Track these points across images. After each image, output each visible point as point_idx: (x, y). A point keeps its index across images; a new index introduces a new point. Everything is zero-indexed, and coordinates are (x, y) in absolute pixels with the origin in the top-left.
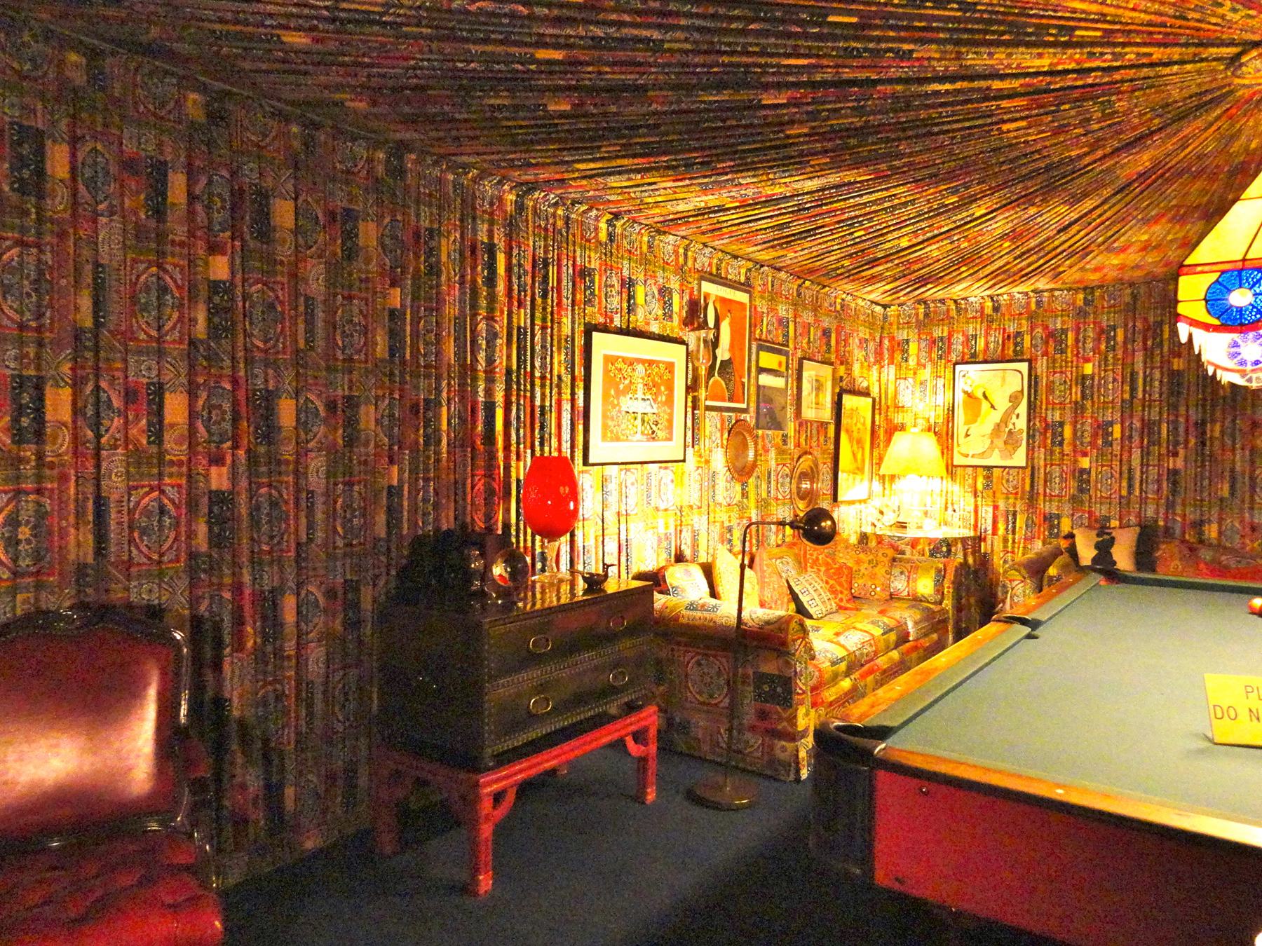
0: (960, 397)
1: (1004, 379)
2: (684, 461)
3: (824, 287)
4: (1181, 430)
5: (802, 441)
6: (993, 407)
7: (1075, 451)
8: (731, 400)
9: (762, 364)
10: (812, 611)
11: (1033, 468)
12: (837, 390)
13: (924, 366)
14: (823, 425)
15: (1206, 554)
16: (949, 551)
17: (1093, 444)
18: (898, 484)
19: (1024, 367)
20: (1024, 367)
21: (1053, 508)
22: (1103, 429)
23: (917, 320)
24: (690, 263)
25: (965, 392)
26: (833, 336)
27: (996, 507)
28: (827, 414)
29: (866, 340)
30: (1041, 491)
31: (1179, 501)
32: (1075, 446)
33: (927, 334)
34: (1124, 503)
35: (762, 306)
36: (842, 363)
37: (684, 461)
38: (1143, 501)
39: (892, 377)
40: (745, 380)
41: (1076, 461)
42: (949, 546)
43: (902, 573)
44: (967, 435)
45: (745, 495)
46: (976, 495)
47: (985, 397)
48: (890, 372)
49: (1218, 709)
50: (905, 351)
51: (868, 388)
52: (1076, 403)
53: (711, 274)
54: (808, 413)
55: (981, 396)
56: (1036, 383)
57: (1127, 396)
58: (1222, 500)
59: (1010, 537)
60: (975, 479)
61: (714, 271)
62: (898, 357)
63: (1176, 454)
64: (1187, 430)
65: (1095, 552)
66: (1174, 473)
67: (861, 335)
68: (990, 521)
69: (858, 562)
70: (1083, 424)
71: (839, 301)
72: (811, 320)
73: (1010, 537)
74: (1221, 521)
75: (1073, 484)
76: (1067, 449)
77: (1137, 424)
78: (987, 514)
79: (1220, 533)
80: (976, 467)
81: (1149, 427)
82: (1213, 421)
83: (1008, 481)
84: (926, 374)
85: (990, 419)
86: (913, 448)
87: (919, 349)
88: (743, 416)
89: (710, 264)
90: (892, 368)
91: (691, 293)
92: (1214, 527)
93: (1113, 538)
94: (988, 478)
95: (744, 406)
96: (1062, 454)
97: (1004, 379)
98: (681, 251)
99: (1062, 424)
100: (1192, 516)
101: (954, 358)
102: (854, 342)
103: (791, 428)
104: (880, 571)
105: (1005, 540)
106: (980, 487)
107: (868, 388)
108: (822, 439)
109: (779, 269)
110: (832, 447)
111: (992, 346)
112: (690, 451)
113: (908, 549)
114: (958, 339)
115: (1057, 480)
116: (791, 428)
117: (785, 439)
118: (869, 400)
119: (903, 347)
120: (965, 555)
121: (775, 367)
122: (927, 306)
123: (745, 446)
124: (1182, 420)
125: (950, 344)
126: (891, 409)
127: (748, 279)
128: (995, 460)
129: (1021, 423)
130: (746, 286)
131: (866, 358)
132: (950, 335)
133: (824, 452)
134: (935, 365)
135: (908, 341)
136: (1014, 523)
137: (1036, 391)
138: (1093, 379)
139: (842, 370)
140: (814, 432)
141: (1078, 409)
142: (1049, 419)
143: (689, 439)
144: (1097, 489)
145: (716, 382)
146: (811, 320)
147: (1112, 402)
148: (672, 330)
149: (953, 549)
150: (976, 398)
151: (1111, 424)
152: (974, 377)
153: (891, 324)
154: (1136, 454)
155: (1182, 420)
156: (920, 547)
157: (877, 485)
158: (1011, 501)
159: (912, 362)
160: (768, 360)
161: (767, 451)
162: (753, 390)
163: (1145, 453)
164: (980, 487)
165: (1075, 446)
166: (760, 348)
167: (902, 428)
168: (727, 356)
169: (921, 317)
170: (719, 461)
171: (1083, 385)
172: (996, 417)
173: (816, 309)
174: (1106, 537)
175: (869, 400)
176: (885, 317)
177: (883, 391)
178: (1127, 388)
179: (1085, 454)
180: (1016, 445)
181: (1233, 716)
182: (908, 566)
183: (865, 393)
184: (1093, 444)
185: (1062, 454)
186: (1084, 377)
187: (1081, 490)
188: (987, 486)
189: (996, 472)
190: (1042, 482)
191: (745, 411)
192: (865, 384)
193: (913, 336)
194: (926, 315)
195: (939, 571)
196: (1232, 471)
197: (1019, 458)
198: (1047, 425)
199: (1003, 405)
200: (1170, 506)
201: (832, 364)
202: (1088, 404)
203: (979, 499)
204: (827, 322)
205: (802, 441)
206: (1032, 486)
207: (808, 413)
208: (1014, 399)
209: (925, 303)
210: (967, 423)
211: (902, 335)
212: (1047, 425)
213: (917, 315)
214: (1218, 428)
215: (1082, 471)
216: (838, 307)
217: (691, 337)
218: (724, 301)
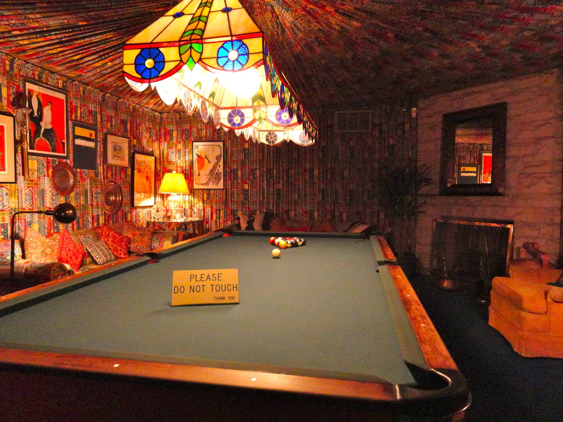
0: (195, 157)
1: (213, 149)
2: (15, 183)
3: (120, 98)
4: (281, 172)
5: (109, 175)
6: (209, 162)
7: (242, 182)
8: (52, 151)
9: (76, 133)
10: (98, 261)
11: (226, 190)
12: (132, 151)
13: (180, 143)
14: (123, 169)
15: (288, 224)
16: (186, 228)
17: (249, 179)
18: (169, 198)
19: (221, 144)
20: (221, 144)
21: (235, 207)
22: (252, 171)
23: (176, 121)
24: (16, 71)
25: (198, 155)
26: (129, 124)
27: (212, 208)
28: (125, 163)
29: (150, 128)
30: (230, 200)
31: (281, 202)
32: (242, 179)
33: (181, 127)
34: (261, 204)
35: (76, 103)
36: (134, 138)
37: (15, 183)
38: (268, 203)
39: (166, 147)
40: (65, 141)
41: (243, 186)
43: (157, 239)
44: (199, 175)
46: (203, 203)
47: (207, 158)
48: (164, 146)
49: (176, 288)
50: (171, 135)
51: (152, 151)
52: (242, 160)
53: (34, 79)
54: (111, 161)
55: (204, 157)
56: (227, 152)
57: (261, 158)
58: (295, 201)
59: (218, 221)
60: (203, 195)
61: (37, 78)
62: (168, 138)
63: (279, 183)
64: (283, 172)
65: (247, 225)
66: (278, 190)
67: (147, 125)
68: (210, 214)
69: (134, 235)
70: (245, 170)
71: (131, 107)
72: (113, 114)
73: (218, 221)
74: (295, 210)
75: (242, 197)
76: (239, 181)
77: (265, 170)
78: (208, 210)
79: (295, 215)
80: (203, 189)
81: (269, 171)
82: (292, 169)
83: (216, 196)
84: (180, 146)
85: (208, 167)
86: (173, 182)
87: (177, 135)
88: (64, 161)
89: (33, 74)
90: (166, 144)
91: (18, 86)
92: (293, 212)
93: (254, 219)
94: (209, 194)
95: (65, 155)
96: (237, 183)
97: (213, 149)
99: (237, 170)
100: (286, 207)
101: (192, 139)
102: (143, 128)
103: (100, 169)
104: (146, 239)
105: (216, 222)
106: (205, 198)
107: (152, 151)
108: (123, 176)
109: (87, 84)
110: (130, 180)
111: (208, 134)
112: (21, 178)
113: (167, 228)
114: (194, 130)
115: (236, 194)
116: (100, 169)
117: (97, 175)
118: (154, 158)
119: (168, 133)
120: (194, 229)
121: (88, 136)
122: (180, 114)
123: (67, 177)
124: (281, 168)
125: (191, 133)
126: (166, 163)
127: (63, 86)
128: (211, 186)
129: (221, 170)
130: (63, 90)
131: (150, 137)
132: (191, 128)
133: (124, 181)
134: (185, 142)
135: (172, 130)
136: (220, 214)
137: (227, 155)
138: (248, 150)
139: (135, 142)
140: (118, 172)
141: (243, 163)
142: (232, 168)
143: (20, 169)
144: (251, 198)
145: (41, 140)
146: (113, 114)
147: (256, 160)
149: (188, 227)
150: (202, 158)
151: (256, 170)
152: (200, 147)
153: (164, 122)
154: (265, 182)
155: (281, 168)
156: (172, 227)
157: (159, 199)
158: (218, 204)
159: (174, 140)
160: (79, 131)
161: (83, 180)
162: (71, 147)
163: (268, 182)
164: (205, 198)
165: (242, 179)
166: (74, 125)
167: (170, 171)
168: (49, 127)
169: (178, 119)
171: (245, 152)
172: (210, 167)
173: (115, 107)
174: (252, 218)
175: (154, 158)
176: (162, 118)
177: (161, 153)
178: (261, 154)
179: (246, 183)
180: (219, 180)
181: (182, 291)
182: (160, 235)
183: (151, 154)
184: (249, 179)
185: (237, 183)
186: (245, 149)
187: (245, 199)
188: (208, 198)
189: (212, 192)
190: (230, 197)
191: (66, 158)
192: (151, 150)
193: (175, 128)
194: (180, 118)
195: (174, 237)
196: (299, 189)
197: (221, 186)
198: (231, 170)
199: (213, 161)
200: (278, 204)
201: (128, 138)
202: (247, 161)
203: (205, 204)
204: (124, 117)
205: (109, 175)
206: (226, 199)
207: (111, 161)
208: (218, 158)
209: (179, 112)
210: (199, 169)
211: (170, 127)
212: (231, 170)
213: (176, 118)
214: (293, 172)
215: (245, 190)
216: (131, 110)
217: (19, 113)
218: (44, 95)
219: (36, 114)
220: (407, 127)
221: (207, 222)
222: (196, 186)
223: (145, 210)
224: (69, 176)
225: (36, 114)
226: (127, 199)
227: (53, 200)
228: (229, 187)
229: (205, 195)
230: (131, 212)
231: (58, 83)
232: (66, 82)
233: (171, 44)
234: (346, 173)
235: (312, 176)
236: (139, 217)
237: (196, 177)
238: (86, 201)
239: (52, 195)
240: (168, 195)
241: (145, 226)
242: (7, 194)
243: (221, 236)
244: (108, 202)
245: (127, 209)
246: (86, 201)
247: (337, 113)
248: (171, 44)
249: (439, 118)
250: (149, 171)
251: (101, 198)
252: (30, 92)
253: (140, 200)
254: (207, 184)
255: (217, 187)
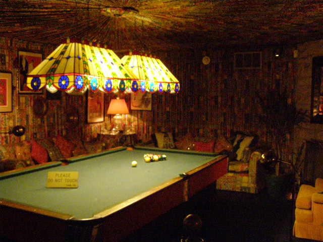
24: (13, 45)
42: (126, 137)
45: (43, 122)
61: (25, 47)
88: (41, 96)
94: (141, 114)
98: (9, 42)
100: (197, 127)
105: (146, 135)
106: (139, 117)
108: (80, 102)
123: (42, 107)
128: (143, 108)
140: (76, 99)
148: (6, 68)
164: (139, 117)
170: (30, 111)
188: (141, 117)
189: (144, 113)
197: (149, 108)
218: (30, 57)
219: (24, 69)
220: (290, 65)
221: (140, 135)
222: (132, 108)
223: (96, 125)
224: (44, 106)
225: (24, 69)
226: (83, 119)
227: (33, 120)
228: (156, 109)
229: (139, 115)
230: (86, 127)
231: (37, 48)
232: (42, 46)
233: (41, 76)
234: (243, 100)
235: (216, 102)
236: (91, 129)
237: (133, 101)
238: (54, 120)
239: (33, 117)
240: (114, 115)
241: (96, 136)
242: (8, 119)
243: (125, 149)
244: (68, 120)
245: (82, 124)
246: (54, 120)
247: (235, 54)
248: (41, 76)
249: (309, 61)
250: (100, 97)
251: (64, 118)
252: (22, 57)
253: (91, 118)
254: (139, 106)
255: (147, 109)
